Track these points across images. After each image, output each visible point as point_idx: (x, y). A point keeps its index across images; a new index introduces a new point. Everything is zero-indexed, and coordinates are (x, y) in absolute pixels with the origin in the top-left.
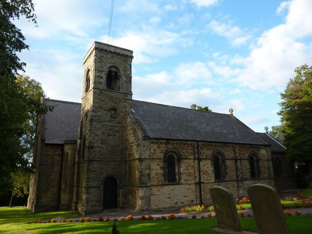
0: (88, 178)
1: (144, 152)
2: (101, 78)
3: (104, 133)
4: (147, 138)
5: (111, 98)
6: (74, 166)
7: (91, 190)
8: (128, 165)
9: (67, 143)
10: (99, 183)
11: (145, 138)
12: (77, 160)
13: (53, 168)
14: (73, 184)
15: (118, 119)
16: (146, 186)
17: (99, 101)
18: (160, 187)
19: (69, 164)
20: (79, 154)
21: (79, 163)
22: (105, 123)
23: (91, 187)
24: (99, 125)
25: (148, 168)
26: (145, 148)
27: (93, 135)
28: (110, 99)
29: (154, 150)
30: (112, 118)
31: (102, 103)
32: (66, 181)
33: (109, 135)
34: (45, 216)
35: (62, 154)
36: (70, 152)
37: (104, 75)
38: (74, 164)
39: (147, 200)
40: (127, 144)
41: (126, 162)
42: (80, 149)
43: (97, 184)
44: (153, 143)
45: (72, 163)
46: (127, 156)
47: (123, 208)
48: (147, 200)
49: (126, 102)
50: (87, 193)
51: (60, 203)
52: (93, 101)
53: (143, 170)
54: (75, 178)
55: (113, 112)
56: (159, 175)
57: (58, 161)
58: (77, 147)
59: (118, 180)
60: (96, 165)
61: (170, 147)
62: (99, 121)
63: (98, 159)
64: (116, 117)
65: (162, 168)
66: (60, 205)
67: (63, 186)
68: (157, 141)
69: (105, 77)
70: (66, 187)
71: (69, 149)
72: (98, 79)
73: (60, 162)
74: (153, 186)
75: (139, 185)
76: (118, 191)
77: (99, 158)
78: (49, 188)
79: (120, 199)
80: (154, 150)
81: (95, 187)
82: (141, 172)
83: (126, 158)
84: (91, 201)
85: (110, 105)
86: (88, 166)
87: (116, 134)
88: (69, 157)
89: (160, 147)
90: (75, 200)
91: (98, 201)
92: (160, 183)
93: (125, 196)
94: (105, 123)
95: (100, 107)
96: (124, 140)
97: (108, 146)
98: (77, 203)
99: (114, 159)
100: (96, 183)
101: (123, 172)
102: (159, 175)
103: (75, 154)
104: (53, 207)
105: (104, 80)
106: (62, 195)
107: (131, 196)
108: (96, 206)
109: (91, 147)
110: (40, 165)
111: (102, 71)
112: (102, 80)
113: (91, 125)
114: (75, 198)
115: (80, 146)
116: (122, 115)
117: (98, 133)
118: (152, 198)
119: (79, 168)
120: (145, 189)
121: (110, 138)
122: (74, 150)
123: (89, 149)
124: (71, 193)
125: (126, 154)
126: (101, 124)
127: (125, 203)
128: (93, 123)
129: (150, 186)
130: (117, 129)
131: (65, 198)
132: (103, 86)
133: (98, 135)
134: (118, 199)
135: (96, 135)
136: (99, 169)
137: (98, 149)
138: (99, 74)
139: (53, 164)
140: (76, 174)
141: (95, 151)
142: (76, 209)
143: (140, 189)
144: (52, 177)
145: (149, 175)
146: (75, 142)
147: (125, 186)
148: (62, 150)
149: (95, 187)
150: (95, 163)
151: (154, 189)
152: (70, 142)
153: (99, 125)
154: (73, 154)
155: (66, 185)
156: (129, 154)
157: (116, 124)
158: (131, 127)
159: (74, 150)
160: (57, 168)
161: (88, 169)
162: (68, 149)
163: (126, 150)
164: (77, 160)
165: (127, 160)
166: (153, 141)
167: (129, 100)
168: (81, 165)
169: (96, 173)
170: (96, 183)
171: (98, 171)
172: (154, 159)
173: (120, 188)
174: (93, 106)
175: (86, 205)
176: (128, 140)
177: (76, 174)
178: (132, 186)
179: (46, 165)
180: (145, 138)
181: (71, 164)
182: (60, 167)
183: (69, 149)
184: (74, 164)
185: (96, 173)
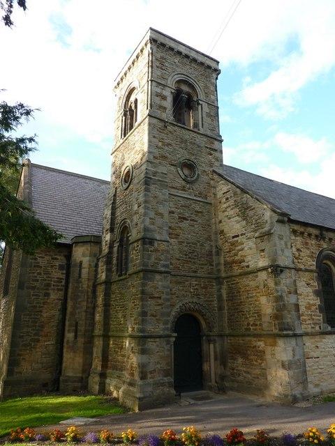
0: (144, 314)
1: (283, 251)
2: (164, 98)
3: (173, 213)
4: (286, 219)
5: (183, 141)
6: (94, 292)
7: (151, 345)
8: (225, 287)
9: (80, 240)
10: (169, 326)
11: (281, 218)
12: (103, 276)
13: (47, 295)
14: (93, 331)
15: (199, 187)
16: (295, 335)
17: (160, 144)
18: (317, 338)
19: (85, 286)
20: (109, 262)
21: (108, 283)
22: (174, 192)
23: (151, 337)
24: (164, 194)
25: (292, 289)
26: (283, 242)
27: (152, 214)
28: (181, 142)
29: (298, 250)
30: (188, 182)
31: (166, 148)
32: (77, 325)
33: (183, 219)
34: (33, 409)
35: (68, 267)
36: (86, 261)
37: (167, 93)
38: (95, 286)
39: (299, 367)
40: (220, 242)
41: (219, 280)
42: (110, 253)
43: (164, 330)
44: (294, 232)
45: (91, 284)
46: (222, 267)
47: (222, 390)
48: (299, 367)
49: (211, 154)
50: (143, 352)
51: (60, 372)
52: (150, 141)
53: (284, 295)
54: (98, 317)
55: (187, 172)
56: (313, 308)
57: (60, 280)
58: (101, 251)
59: (203, 322)
60: (159, 282)
61: (325, 246)
62: (163, 184)
63: (163, 269)
64: (197, 179)
65: (317, 293)
66: (61, 378)
67: (69, 336)
68: (302, 230)
69: (170, 99)
70: (76, 337)
71: (84, 255)
72: (157, 100)
73: (64, 281)
74: (307, 334)
75: (277, 331)
76: (205, 347)
77: (164, 266)
78: (38, 341)
79: (211, 367)
80: (298, 250)
81: (160, 337)
82: (279, 299)
83: (219, 271)
84: (151, 372)
85: (182, 155)
86: (143, 285)
87: (196, 218)
88: (85, 271)
89: (307, 244)
90: (99, 368)
91: (166, 374)
92: (317, 328)
93: (223, 360)
94: (174, 192)
95: (164, 157)
96: (213, 234)
97: (181, 243)
98: (103, 376)
99: (195, 272)
100: (162, 326)
101: (215, 304)
102: (313, 308)
103: (97, 266)
104: (45, 385)
105: (168, 103)
106: (67, 356)
107: (240, 360)
108: (163, 384)
109: (147, 241)
110: (21, 286)
111: (164, 86)
112: (165, 104)
113: (147, 190)
114: (97, 364)
115: (111, 247)
116: (204, 178)
117: (161, 209)
118: (309, 362)
119: (107, 295)
120: (293, 341)
121: (185, 224)
122: (95, 256)
123: (144, 243)
124: (88, 351)
125: (219, 264)
126: (166, 191)
127: (223, 378)
128: (152, 187)
129: (301, 336)
130: (197, 208)
131: (72, 363)
132: (168, 115)
133: (161, 215)
134: (206, 367)
135: (158, 214)
136: (167, 294)
137: (163, 246)
138: (159, 90)
139: (49, 285)
140: (100, 309)
141: (156, 250)
142: (103, 390)
143: (281, 342)
144: (45, 315)
145: (297, 306)
146: (96, 241)
147: (221, 336)
148: (69, 257)
149: (160, 337)
150: (158, 277)
151: (309, 342)
152: (85, 239)
153: (164, 194)
154: (93, 264)
155: (76, 332)
156: (226, 263)
157: (195, 196)
158: (231, 202)
159: (96, 257)
160: (55, 296)
161: (143, 292)
162: (81, 254)
163: (218, 254)
164: (103, 276)
165: (223, 275)
166: (296, 227)
167: (216, 150)
168: (114, 287)
169: (160, 301)
170: (162, 326)
171: (164, 296)
172: (301, 270)
173: (209, 341)
174: (149, 152)
175: (140, 382)
176: (222, 232)
177: (100, 309)
178: (243, 336)
179: (33, 288)
180: (281, 218)
181: (88, 287)
182: (62, 293)
183: (84, 255)
184: (95, 286)
185: (160, 301)
